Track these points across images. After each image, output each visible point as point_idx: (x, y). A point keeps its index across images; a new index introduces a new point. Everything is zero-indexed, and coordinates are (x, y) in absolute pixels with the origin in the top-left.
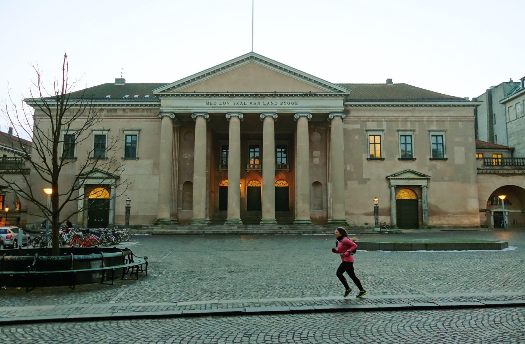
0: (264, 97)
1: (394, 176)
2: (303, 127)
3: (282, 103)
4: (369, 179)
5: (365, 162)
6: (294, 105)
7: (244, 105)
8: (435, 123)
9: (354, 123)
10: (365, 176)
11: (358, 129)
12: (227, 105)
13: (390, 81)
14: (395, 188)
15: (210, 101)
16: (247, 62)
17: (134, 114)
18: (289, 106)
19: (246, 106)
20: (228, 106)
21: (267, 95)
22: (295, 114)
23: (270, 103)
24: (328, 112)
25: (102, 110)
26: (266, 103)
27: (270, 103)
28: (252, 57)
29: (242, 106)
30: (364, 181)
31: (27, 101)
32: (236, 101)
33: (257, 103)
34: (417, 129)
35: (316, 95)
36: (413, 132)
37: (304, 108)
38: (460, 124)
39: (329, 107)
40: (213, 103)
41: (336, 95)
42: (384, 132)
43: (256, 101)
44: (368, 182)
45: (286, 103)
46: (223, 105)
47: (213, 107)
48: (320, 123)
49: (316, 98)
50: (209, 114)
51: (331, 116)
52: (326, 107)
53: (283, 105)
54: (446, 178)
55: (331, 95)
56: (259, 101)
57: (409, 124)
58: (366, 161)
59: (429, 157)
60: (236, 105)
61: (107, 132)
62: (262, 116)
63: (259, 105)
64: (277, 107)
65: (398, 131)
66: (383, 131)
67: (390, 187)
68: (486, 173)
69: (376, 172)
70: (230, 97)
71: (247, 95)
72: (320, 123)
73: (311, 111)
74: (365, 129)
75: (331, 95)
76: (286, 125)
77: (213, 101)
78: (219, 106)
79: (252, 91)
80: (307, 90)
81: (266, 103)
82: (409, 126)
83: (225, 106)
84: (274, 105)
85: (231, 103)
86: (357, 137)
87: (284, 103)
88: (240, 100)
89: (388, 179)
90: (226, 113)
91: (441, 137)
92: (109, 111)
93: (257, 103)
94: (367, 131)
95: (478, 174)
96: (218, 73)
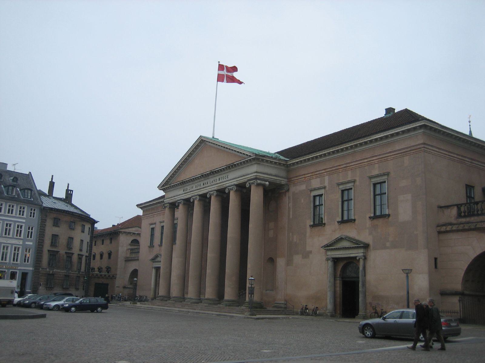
5: (308, 229)
6: (227, 179)
10: (308, 249)
15: (186, 188)
31: (137, 206)
39: (246, 175)
44: (311, 256)
54: (388, 244)
68: (458, 231)
69: (316, 241)
84: (215, 183)
86: (302, 201)
95: (440, 233)
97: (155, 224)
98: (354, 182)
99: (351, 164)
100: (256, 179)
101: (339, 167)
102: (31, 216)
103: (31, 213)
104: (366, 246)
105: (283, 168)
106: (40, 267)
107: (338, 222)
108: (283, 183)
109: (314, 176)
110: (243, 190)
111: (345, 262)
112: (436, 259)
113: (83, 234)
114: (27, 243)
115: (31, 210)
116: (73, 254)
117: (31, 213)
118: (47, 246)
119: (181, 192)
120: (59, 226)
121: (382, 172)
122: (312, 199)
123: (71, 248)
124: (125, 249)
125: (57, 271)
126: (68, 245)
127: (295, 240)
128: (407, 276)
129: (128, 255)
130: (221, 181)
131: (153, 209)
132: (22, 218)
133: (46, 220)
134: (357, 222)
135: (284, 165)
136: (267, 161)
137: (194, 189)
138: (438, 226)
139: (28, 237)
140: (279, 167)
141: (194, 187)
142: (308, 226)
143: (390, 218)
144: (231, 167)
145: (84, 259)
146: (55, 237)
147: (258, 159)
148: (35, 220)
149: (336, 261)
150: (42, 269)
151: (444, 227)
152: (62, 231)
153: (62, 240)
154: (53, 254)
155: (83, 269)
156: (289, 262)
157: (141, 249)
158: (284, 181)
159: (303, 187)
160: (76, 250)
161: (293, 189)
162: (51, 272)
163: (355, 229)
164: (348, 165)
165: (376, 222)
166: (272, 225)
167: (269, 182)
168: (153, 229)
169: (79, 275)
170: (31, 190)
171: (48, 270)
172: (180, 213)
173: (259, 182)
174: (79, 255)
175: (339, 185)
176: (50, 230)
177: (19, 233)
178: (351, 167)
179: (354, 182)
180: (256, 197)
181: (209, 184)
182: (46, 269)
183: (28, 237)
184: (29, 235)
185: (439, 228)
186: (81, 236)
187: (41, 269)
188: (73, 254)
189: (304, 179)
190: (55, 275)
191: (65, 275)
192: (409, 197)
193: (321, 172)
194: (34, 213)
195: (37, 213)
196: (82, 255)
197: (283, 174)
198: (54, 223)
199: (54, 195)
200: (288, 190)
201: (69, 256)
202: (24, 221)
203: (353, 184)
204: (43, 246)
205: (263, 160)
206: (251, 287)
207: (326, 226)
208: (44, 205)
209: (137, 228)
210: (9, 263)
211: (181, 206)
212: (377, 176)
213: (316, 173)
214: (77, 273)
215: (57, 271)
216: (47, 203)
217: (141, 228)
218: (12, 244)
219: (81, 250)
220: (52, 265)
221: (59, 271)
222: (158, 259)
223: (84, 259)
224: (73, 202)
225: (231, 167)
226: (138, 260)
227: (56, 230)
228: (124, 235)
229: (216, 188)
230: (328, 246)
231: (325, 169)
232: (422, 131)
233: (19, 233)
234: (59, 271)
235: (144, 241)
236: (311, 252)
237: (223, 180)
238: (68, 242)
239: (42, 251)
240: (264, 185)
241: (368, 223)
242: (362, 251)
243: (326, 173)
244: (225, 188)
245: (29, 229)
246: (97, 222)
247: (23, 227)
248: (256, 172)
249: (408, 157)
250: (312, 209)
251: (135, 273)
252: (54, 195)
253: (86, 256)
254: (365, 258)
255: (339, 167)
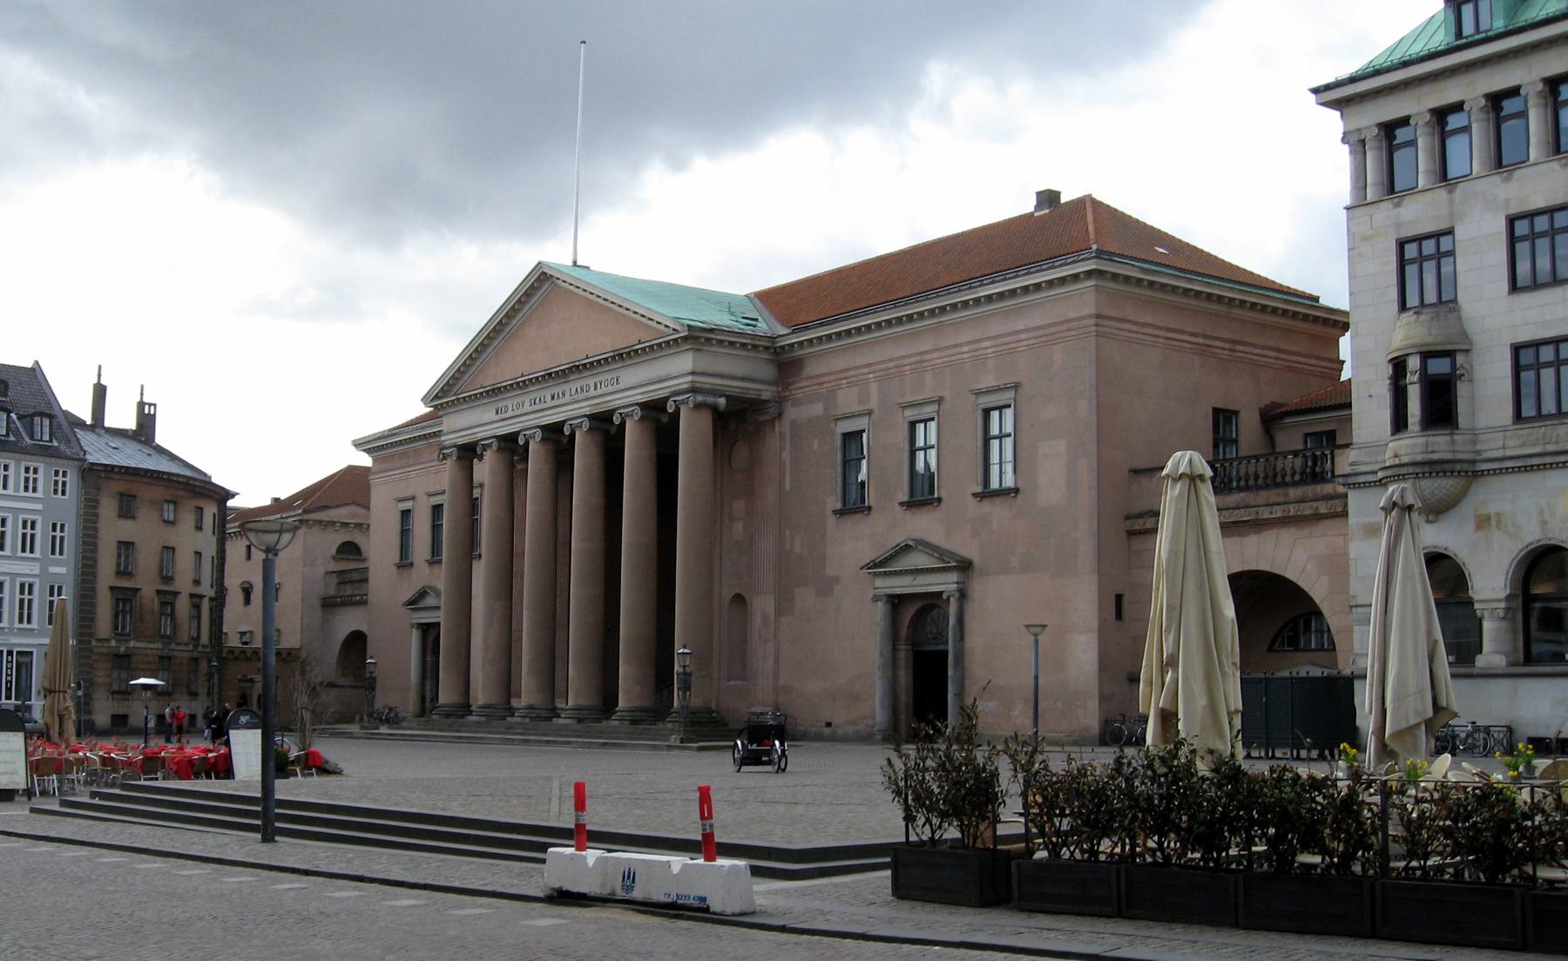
5: (831, 520)
6: (616, 387)
10: (831, 571)
13: (1048, 198)
15: (501, 404)
31: (358, 444)
42: (874, 417)
84: (585, 395)
86: (816, 446)
88: (536, 393)
97: (413, 498)
98: (940, 401)
100: (693, 390)
102: (56, 492)
103: (56, 482)
104: (965, 566)
105: (765, 356)
106: (92, 635)
107: (901, 504)
108: (765, 396)
110: (660, 420)
111: (919, 604)
112: (1119, 598)
113: (199, 534)
114: (52, 570)
115: (57, 473)
116: (176, 594)
117: (56, 482)
118: (106, 576)
119: (490, 415)
120: (133, 518)
121: (1001, 382)
122: (838, 441)
123: (172, 579)
124: (322, 571)
125: (138, 645)
126: (161, 570)
127: (798, 549)
128: (1036, 641)
129: (332, 592)
130: (599, 391)
131: (404, 454)
132: (29, 496)
133: (97, 501)
135: (767, 348)
136: (721, 342)
137: (527, 408)
138: (1128, 518)
139: (53, 553)
140: (752, 354)
141: (527, 403)
142: (829, 512)
144: (624, 356)
145: (205, 605)
146: (126, 547)
147: (697, 338)
148: (68, 505)
149: (896, 602)
150: (99, 640)
151: (1141, 521)
152: (144, 530)
153: (147, 560)
154: (124, 598)
155: (205, 639)
156: (784, 605)
157: (372, 575)
158: (767, 393)
159: (817, 409)
160: (183, 584)
161: (791, 412)
162: (122, 649)
165: (987, 506)
166: (739, 506)
167: (729, 398)
168: (406, 514)
169: (196, 655)
170: (51, 417)
171: (113, 643)
172: (485, 470)
173: (700, 398)
174: (192, 596)
175: (905, 407)
176: (112, 529)
177: (28, 543)
179: (940, 401)
180: (692, 434)
181: (567, 398)
182: (108, 640)
183: (53, 553)
184: (55, 546)
185: (1129, 523)
186: (193, 540)
187: (94, 643)
188: (176, 594)
190: (134, 659)
191: (161, 658)
192: (1061, 446)
194: (64, 484)
195: (72, 479)
196: (201, 597)
197: (768, 372)
198: (121, 508)
199: (107, 424)
200: (780, 415)
201: (167, 599)
202: (39, 507)
203: (935, 407)
204: (95, 575)
205: (708, 340)
206: (685, 673)
207: (873, 512)
208: (91, 459)
209: (353, 509)
210: (11, 628)
211: (488, 455)
212: (989, 391)
214: (191, 647)
215: (138, 645)
216: (98, 452)
217: (368, 508)
218: (14, 575)
219: (197, 582)
220: (123, 628)
221: (142, 645)
222: (430, 601)
223: (205, 605)
224: (161, 439)
225: (624, 356)
226: (365, 603)
227: (128, 530)
228: (315, 529)
229: (587, 411)
230: (876, 565)
231: (870, 365)
232: (1092, 283)
233: (28, 543)
234: (142, 645)
235: (380, 548)
236: (836, 580)
237: (604, 390)
238: (162, 560)
239: (94, 590)
240: (714, 409)
242: (953, 577)
244: (612, 412)
245: (54, 529)
246: (233, 495)
247: (39, 526)
248: (693, 373)
250: (839, 470)
251: (356, 642)
252: (107, 424)
253: (211, 599)
254: (963, 595)
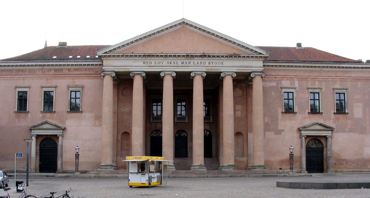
0: (194, 57)
1: (305, 128)
2: (228, 85)
3: (209, 64)
4: (283, 130)
5: (280, 115)
6: (221, 65)
7: (176, 65)
8: (338, 83)
9: (271, 81)
11: (274, 86)
12: (161, 64)
14: (305, 138)
15: (146, 61)
16: (179, 26)
17: (77, 73)
18: (216, 65)
19: (178, 65)
20: (162, 65)
21: (197, 56)
22: (221, 72)
23: (199, 63)
24: (250, 71)
25: (50, 70)
26: (196, 62)
27: (199, 63)
28: (183, 22)
29: (174, 65)
30: (279, 132)
32: (169, 61)
33: (188, 63)
34: (324, 88)
35: (239, 57)
36: (320, 90)
37: (229, 68)
38: (359, 84)
40: (149, 63)
41: (257, 57)
42: (297, 89)
43: (187, 61)
44: (283, 133)
45: (214, 63)
46: (158, 65)
47: (149, 66)
48: (243, 82)
49: (239, 59)
50: (145, 72)
51: (252, 75)
52: (248, 67)
53: (211, 65)
54: (347, 130)
55: (252, 57)
56: (189, 61)
57: (317, 82)
58: (281, 114)
59: (333, 112)
60: (169, 65)
61: (54, 89)
62: (192, 75)
63: (189, 65)
64: (206, 67)
65: (308, 89)
66: (295, 88)
67: (301, 137)
70: (164, 57)
71: (179, 56)
72: (243, 82)
73: (235, 71)
74: (280, 86)
75: (252, 57)
76: (213, 83)
77: (149, 61)
78: (153, 66)
79: (184, 53)
80: (231, 52)
81: (196, 62)
82: (317, 85)
83: (159, 65)
85: (165, 63)
86: (273, 94)
87: (211, 63)
88: (172, 60)
89: (299, 130)
90: (161, 72)
91: (343, 94)
92: (56, 70)
93: (188, 63)
94: (282, 88)
96: (153, 36)
98: (321, 89)
99: (319, 77)
101: (309, 77)
104: (331, 129)
109: (284, 78)
111: (311, 138)
119: (141, 63)
134: (323, 114)
143: (348, 115)
163: (323, 119)
164: (317, 77)
178: (318, 79)
189: (274, 78)
192: (361, 105)
193: (292, 77)
207: (297, 114)
213: (287, 77)
231: (296, 76)
241: (333, 116)
243: (296, 79)
249: (360, 82)
255: (309, 77)
